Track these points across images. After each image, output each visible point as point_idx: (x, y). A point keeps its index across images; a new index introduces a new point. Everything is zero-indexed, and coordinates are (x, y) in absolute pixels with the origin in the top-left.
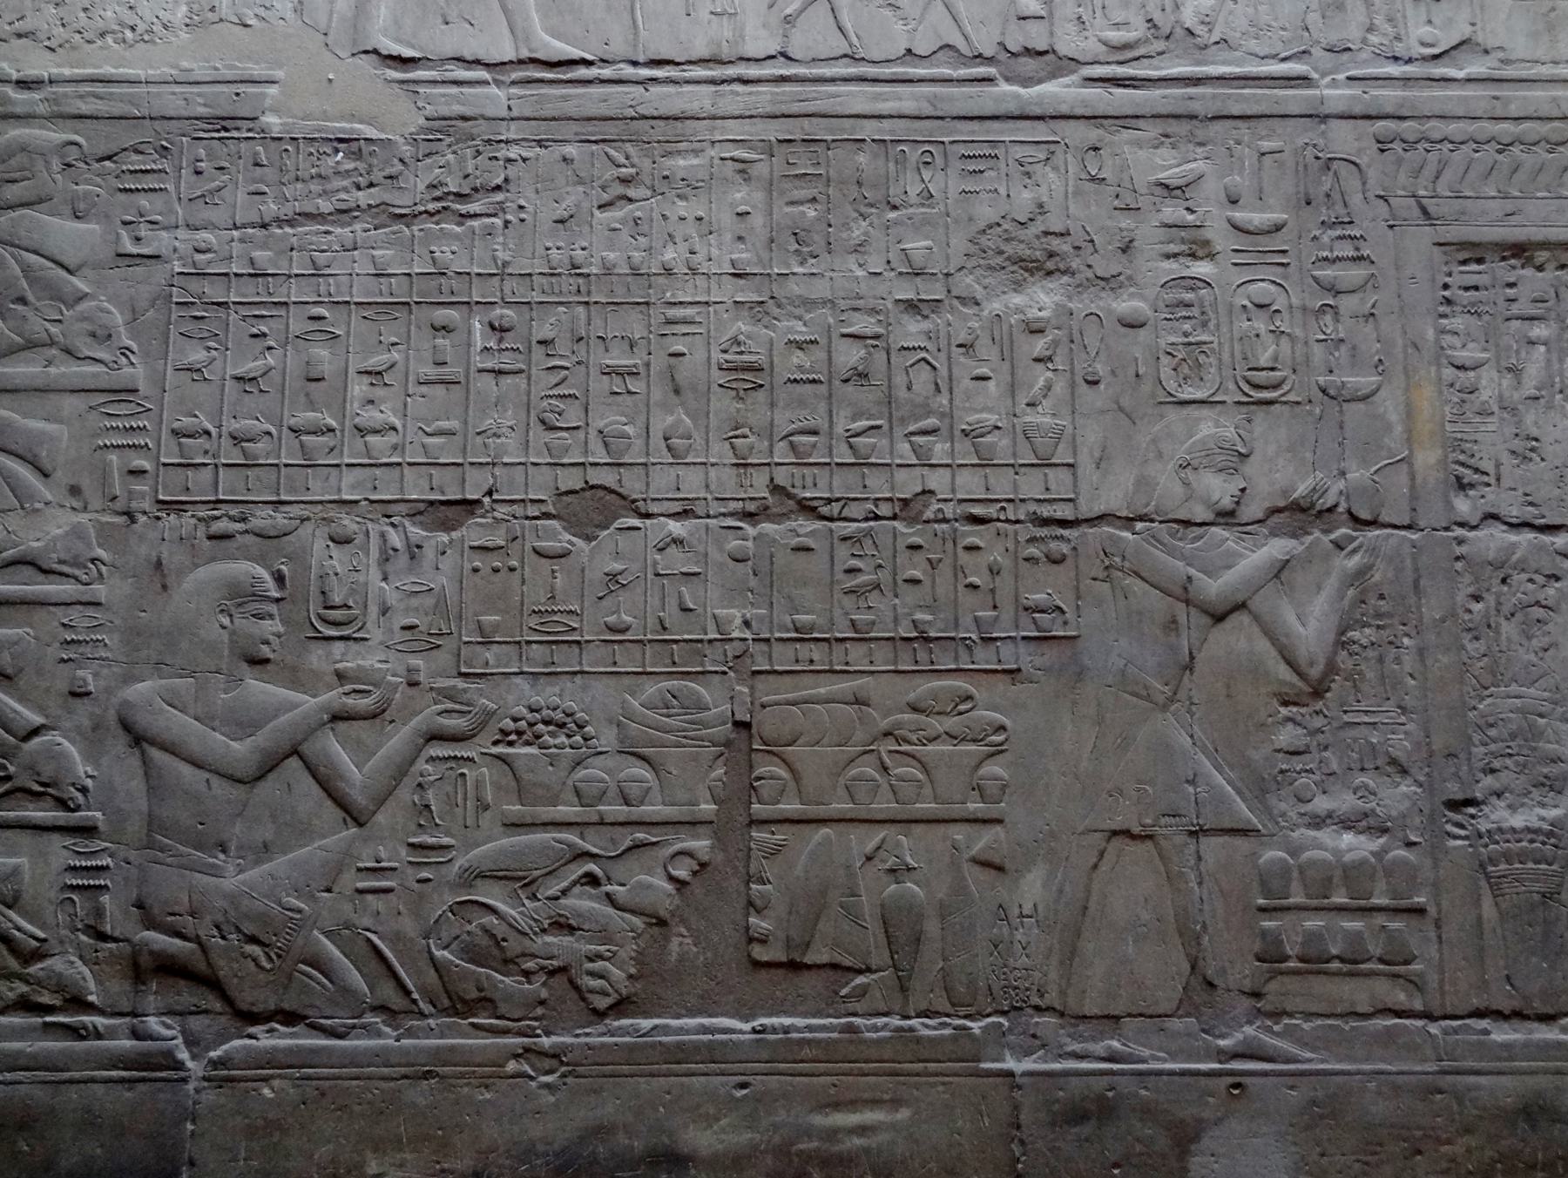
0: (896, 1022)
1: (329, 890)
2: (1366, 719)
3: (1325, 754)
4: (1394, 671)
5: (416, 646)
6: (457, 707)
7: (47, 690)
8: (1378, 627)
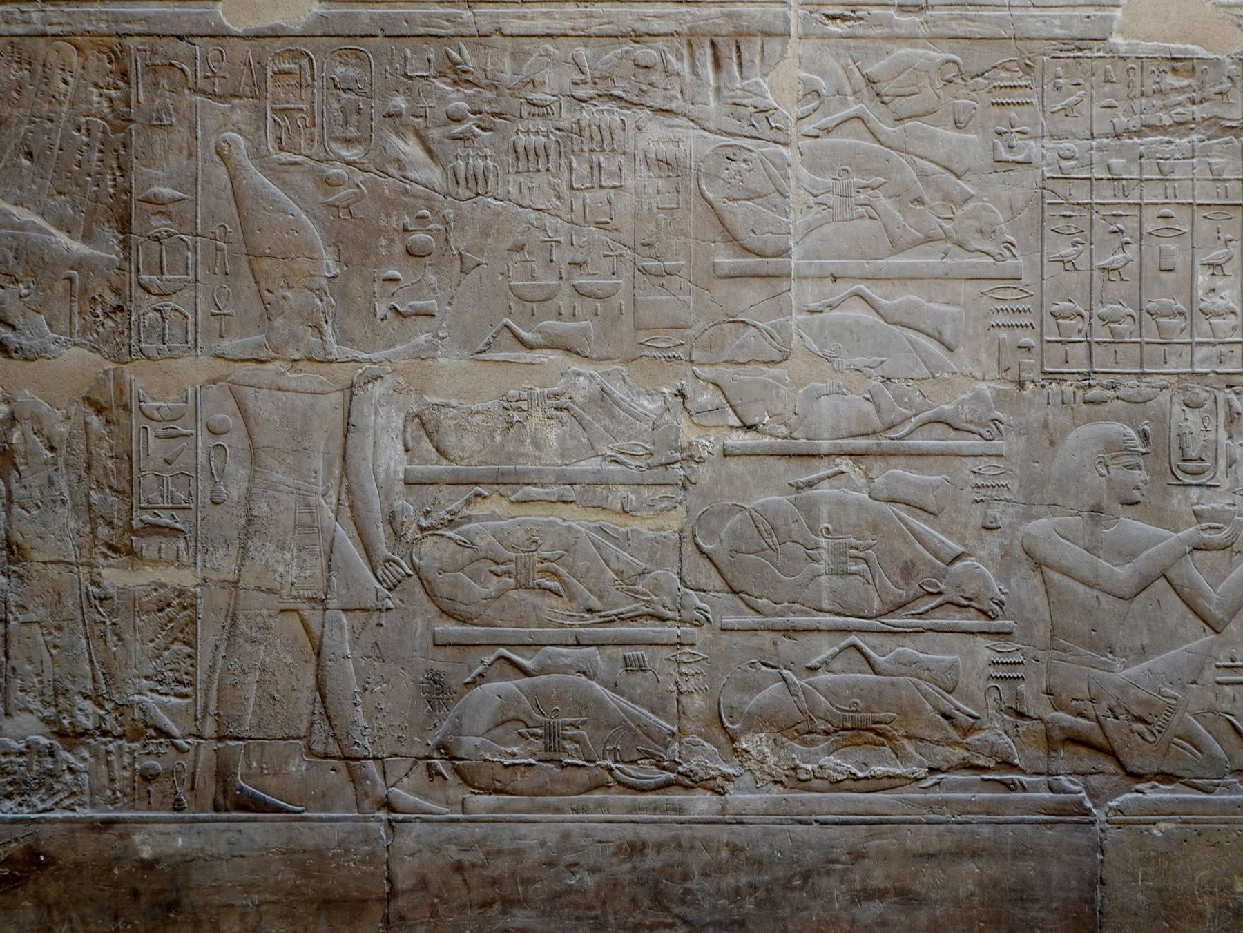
1: (1194, 682)
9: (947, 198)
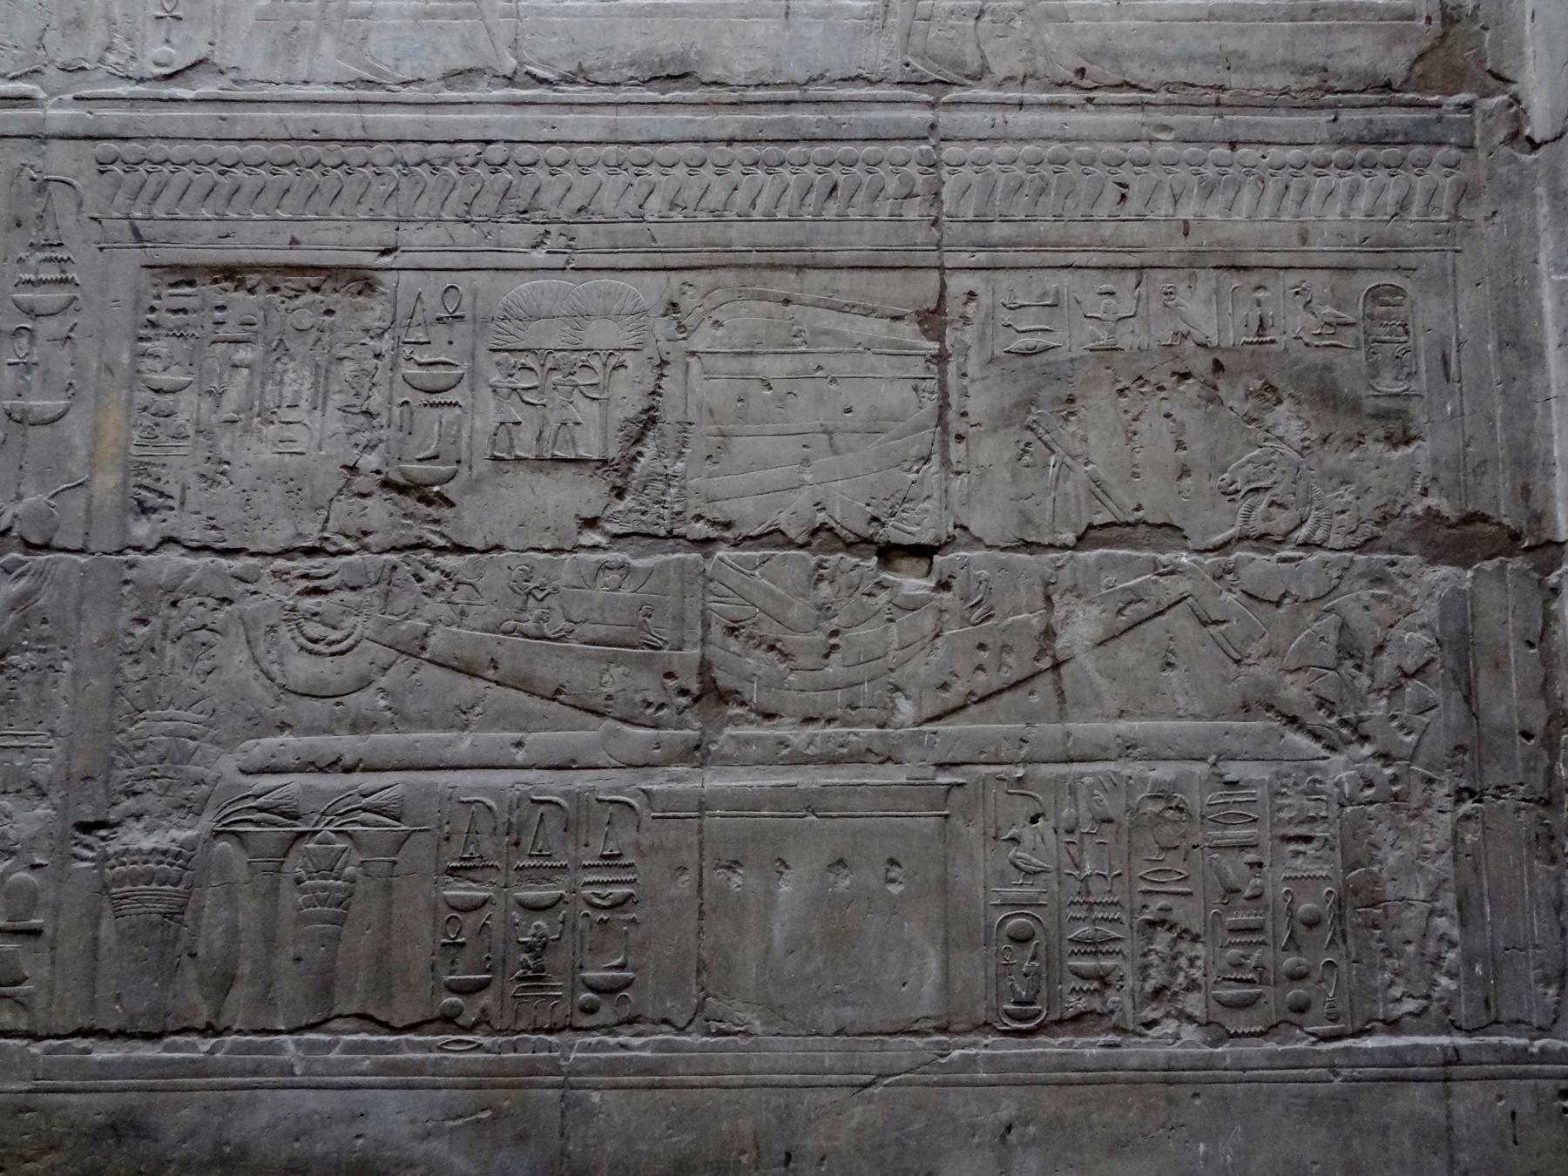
2: (16, 743)
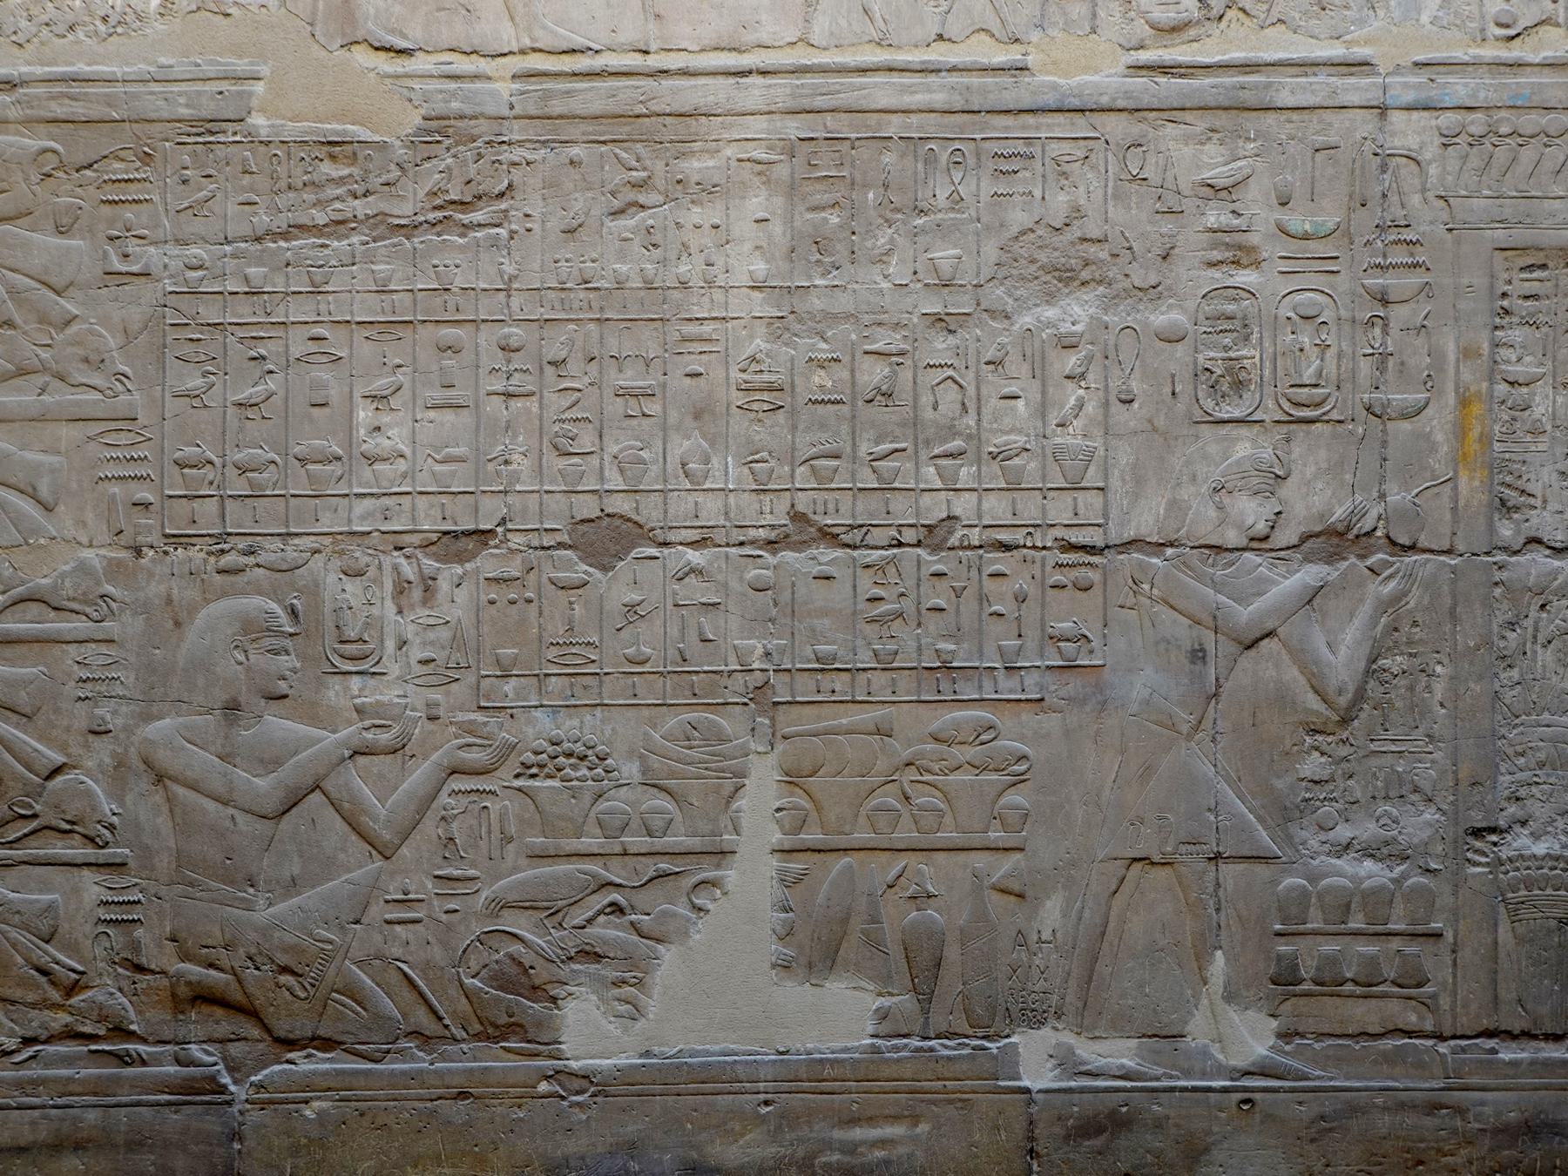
0: (915, 1042)
1: (357, 922)
3: (1351, 782)
4: (1423, 699)
5: (434, 680)
6: (479, 741)
7: (68, 729)
8: (1411, 655)
9: (43, 319)
